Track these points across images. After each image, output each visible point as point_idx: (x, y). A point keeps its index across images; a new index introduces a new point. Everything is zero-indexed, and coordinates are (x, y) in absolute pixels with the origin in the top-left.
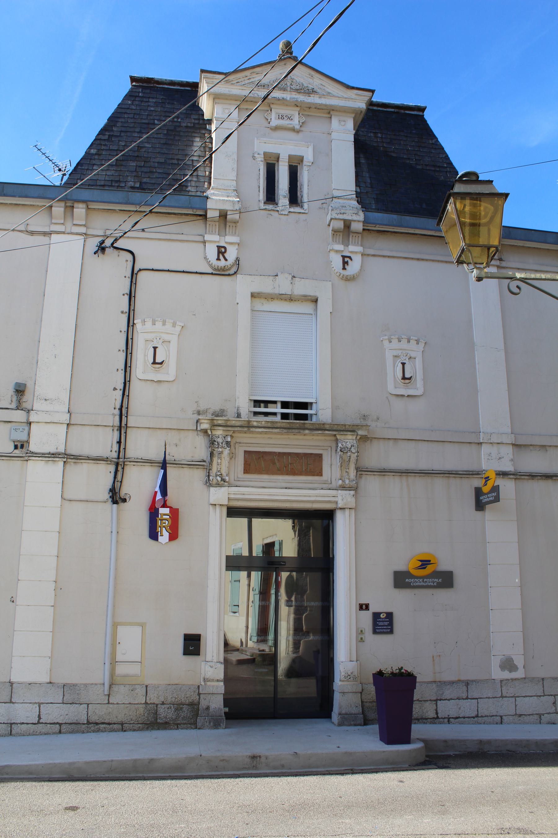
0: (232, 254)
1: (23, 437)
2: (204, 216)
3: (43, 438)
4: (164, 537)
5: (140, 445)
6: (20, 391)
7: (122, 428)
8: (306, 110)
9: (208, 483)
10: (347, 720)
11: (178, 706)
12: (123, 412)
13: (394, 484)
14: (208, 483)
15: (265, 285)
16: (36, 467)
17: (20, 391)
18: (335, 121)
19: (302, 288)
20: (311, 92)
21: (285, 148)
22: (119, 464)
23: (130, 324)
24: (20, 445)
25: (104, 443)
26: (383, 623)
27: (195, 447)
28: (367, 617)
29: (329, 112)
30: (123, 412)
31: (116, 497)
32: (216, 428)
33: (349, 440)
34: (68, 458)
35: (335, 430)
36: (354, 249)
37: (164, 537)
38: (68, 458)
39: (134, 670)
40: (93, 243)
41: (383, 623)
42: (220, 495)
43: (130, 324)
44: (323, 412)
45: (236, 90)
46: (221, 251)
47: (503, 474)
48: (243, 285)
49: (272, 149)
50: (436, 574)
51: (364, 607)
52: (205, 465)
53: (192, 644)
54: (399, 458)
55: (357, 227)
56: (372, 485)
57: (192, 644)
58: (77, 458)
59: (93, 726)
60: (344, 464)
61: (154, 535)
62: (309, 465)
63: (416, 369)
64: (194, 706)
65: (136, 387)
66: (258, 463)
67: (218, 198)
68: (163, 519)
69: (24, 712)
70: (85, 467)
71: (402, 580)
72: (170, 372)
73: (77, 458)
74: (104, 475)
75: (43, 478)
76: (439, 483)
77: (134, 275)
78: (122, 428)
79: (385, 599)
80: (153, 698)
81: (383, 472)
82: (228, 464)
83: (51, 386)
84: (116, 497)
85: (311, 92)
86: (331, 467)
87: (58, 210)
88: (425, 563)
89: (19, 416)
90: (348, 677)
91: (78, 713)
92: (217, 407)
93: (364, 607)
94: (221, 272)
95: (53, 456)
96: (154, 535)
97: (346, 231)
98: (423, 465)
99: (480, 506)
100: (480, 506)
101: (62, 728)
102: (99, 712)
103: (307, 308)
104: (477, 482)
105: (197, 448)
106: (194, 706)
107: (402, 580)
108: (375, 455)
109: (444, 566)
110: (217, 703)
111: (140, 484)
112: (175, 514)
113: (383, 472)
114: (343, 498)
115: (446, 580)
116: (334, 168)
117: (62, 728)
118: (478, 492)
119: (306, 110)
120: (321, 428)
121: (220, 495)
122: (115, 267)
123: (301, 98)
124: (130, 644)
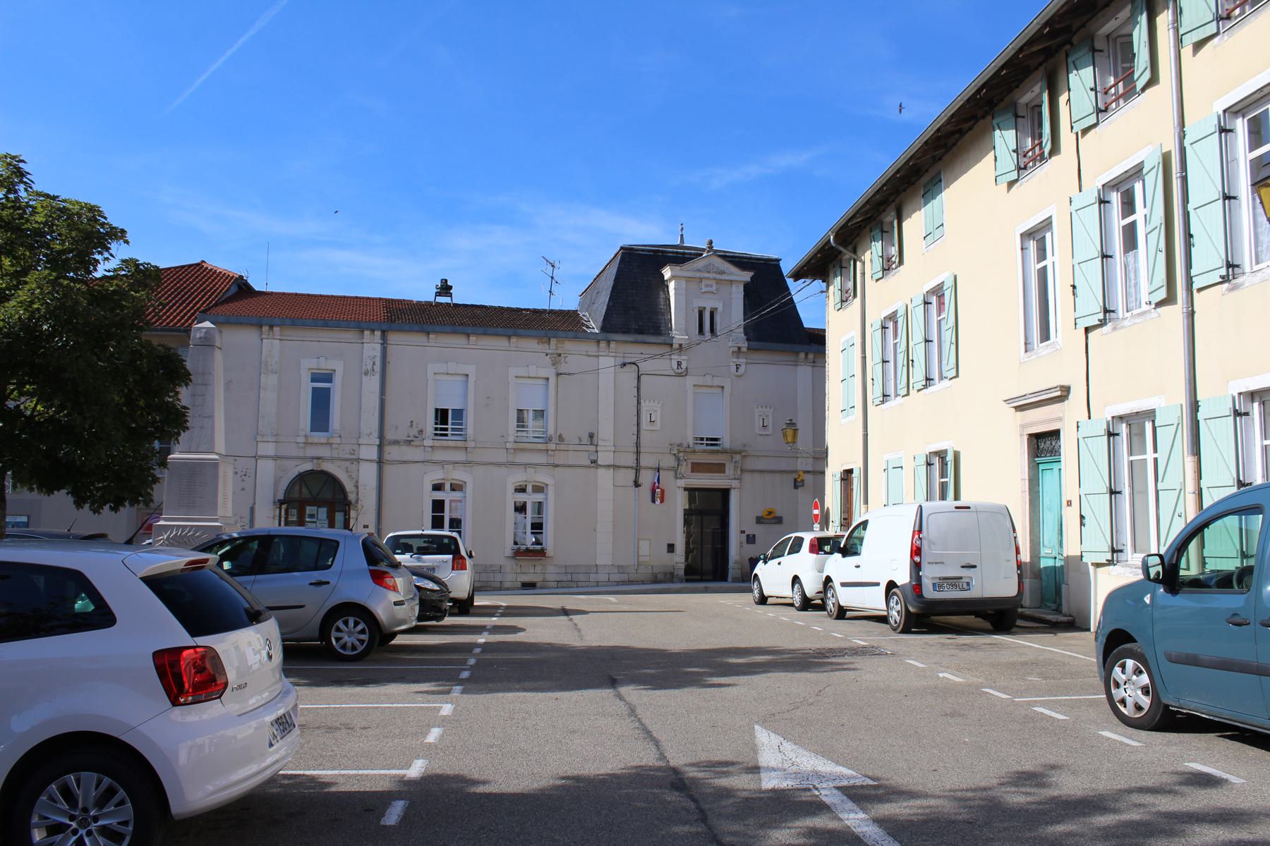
0: (684, 365)
1: (594, 458)
2: (671, 345)
3: (604, 458)
4: (658, 502)
5: (645, 461)
6: (591, 436)
7: (638, 453)
8: (718, 281)
9: (676, 478)
10: (735, 580)
11: (665, 574)
12: (638, 445)
13: (757, 476)
14: (676, 478)
15: (700, 381)
16: (601, 471)
17: (591, 436)
18: (734, 288)
19: (717, 381)
20: (722, 273)
21: (708, 305)
22: (638, 470)
23: (639, 403)
24: (594, 462)
25: (630, 460)
26: (751, 539)
27: (669, 461)
28: (744, 536)
29: (731, 282)
30: (638, 445)
31: (637, 484)
32: (680, 452)
33: (738, 457)
34: (615, 467)
35: (731, 452)
36: (742, 360)
37: (658, 502)
38: (615, 467)
39: (647, 559)
40: (620, 361)
41: (751, 539)
42: (682, 483)
43: (639, 403)
44: (726, 443)
45: (685, 274)
46: (679, 364)
47: (808, 472)
48: (690, 381)
49: (702, 305)
50: (775, 518)
51: (743, 532)
52: (675, 470)
53: (671, 548)
54: (760, 464)
55: (744, 349)
56: (747, 477)
57: (671, 548)
58: (619, 467)
59: (631, 582)
60: (735, 468)
61: (654, 501)
62: (719, 468)
63: (769, 422)
64: (672, 574)
65: (643, 433)
66: (697, 468)
67: (678, 336)
68: (657, 494)
69: (603, 577)
70: (622, 470)
71: (759, 520)
72: (658, 426)
73: (619, 467)
74: (631, 475)
75: (605, 476)
76: (778, 476)
77: (639, 377)
78: (638, 453)
79: (753, 528)
80: (655, 570)
81: (753, 471)
82: (685, 469)
83: (606, 433)
84: (637, 484)
85: (722, 273)
86: (729, 469)
87: (603, 345)
88: (770, 513)
89: (592, 448)
90: (736, 562)
91: (625, 577)
92: (679, 442)
93: (743, 532)
94: (679, 375)
95: (609, 466)
96: (654, 501)
97: (739, 351)
98: (771, 468)
99: (796, 487)
100: (796, 487)
101: (618, 583)
102: (633, 577)
103: (719, 390)
104: (795, 476)
105: (672, 462)
106: (672, 574)
107: (759, 520)
108: (749, 464)
109: (778, 514)
110: (682, 572)
111: (647, 478)
112: (663, 491)
113: (753, 471)
114: (735, 483)
115: (779, 520)
116: (733, 312)
117: (618, 583)
118: (795, 480)
119: (718, 281)
120: (724, 452)
121: (682, 483)
122: (630, 374)
123: (718, 276)
124: (645, 547)
